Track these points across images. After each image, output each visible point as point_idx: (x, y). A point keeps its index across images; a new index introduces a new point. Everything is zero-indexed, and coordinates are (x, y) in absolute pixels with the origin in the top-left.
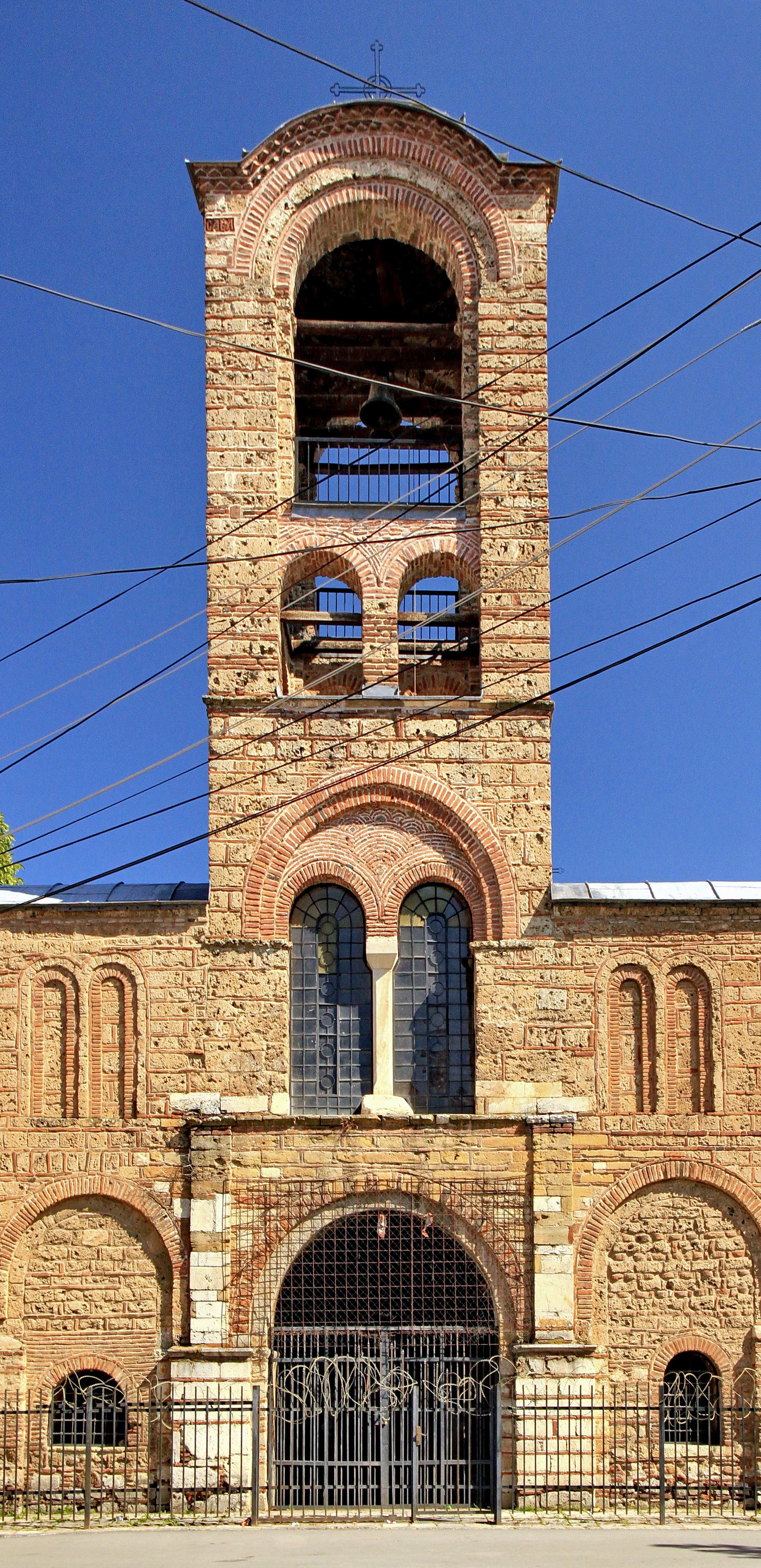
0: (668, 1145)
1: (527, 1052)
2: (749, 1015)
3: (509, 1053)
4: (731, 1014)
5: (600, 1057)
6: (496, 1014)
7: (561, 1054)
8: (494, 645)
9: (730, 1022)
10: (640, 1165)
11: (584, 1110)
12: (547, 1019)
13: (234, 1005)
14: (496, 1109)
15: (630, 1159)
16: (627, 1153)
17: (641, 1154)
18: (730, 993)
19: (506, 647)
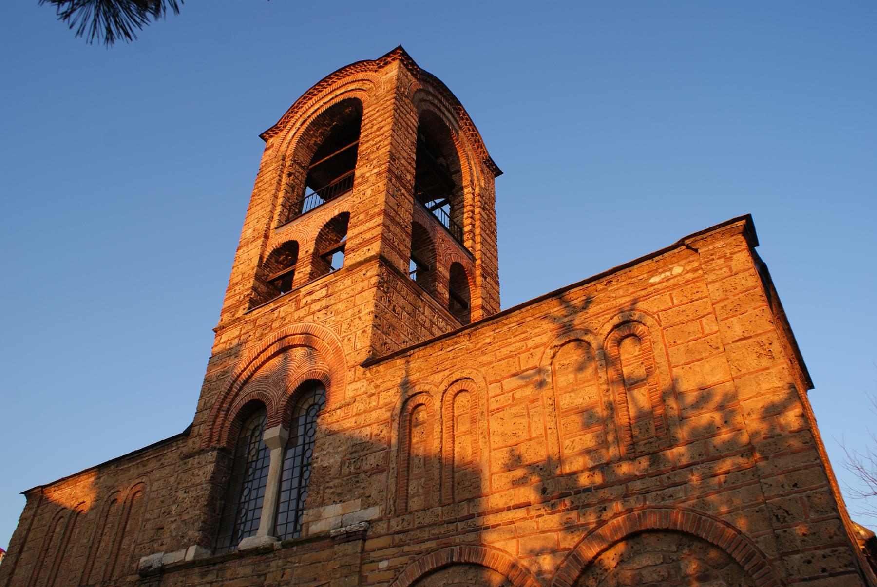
0: (441, 533)
1: (340, 481)
2: (510, 402)
3: (327, 485)
4: (494, 406)
5: (391, 471)
6: (324, 458)
7: (363, 476)
8: (352, 241)
9: (492, 412)
10: (417, 557)
11: (376, 517)
12: (355, 452)
13: (185, 492)
14: (316, 528)
15: (408, 553)
16: (406, 548)
17: (417, 548)
18: (494, 389)
19: (359, 238)
